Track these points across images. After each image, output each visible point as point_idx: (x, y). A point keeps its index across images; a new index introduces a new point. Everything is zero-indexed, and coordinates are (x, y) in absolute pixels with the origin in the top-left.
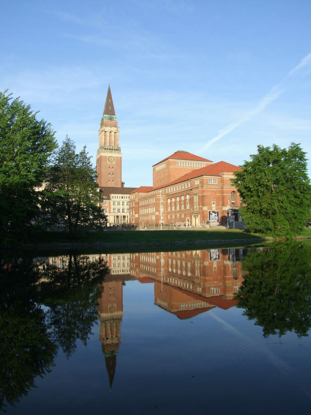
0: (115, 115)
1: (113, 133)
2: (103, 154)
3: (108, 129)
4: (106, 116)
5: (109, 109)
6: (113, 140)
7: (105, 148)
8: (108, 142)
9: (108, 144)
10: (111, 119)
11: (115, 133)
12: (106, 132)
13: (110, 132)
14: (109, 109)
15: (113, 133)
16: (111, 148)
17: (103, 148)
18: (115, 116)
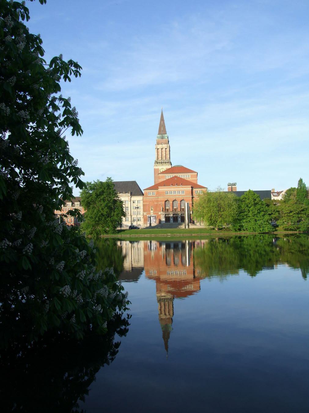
0: (166, 134)
1: (164, 150)
2: (156, 168)
3: (160, 146)
4: (159, 136)
5: (162, 130)
6: (164, 155)
7: (157, 162)
8: (160, 157)
9: (160, 159)
10: (162, 138)
11: (166, 148)
12: (158, 149)
13: (162, 149)
14: (162, 130)
15: (164, 150)
16: (163, 161)
17: (157, 162)
18: (166, 135)
